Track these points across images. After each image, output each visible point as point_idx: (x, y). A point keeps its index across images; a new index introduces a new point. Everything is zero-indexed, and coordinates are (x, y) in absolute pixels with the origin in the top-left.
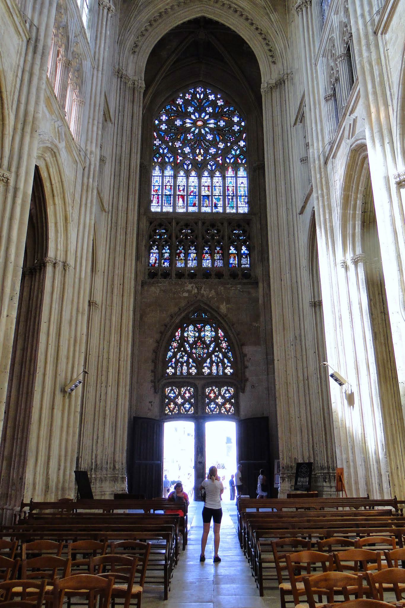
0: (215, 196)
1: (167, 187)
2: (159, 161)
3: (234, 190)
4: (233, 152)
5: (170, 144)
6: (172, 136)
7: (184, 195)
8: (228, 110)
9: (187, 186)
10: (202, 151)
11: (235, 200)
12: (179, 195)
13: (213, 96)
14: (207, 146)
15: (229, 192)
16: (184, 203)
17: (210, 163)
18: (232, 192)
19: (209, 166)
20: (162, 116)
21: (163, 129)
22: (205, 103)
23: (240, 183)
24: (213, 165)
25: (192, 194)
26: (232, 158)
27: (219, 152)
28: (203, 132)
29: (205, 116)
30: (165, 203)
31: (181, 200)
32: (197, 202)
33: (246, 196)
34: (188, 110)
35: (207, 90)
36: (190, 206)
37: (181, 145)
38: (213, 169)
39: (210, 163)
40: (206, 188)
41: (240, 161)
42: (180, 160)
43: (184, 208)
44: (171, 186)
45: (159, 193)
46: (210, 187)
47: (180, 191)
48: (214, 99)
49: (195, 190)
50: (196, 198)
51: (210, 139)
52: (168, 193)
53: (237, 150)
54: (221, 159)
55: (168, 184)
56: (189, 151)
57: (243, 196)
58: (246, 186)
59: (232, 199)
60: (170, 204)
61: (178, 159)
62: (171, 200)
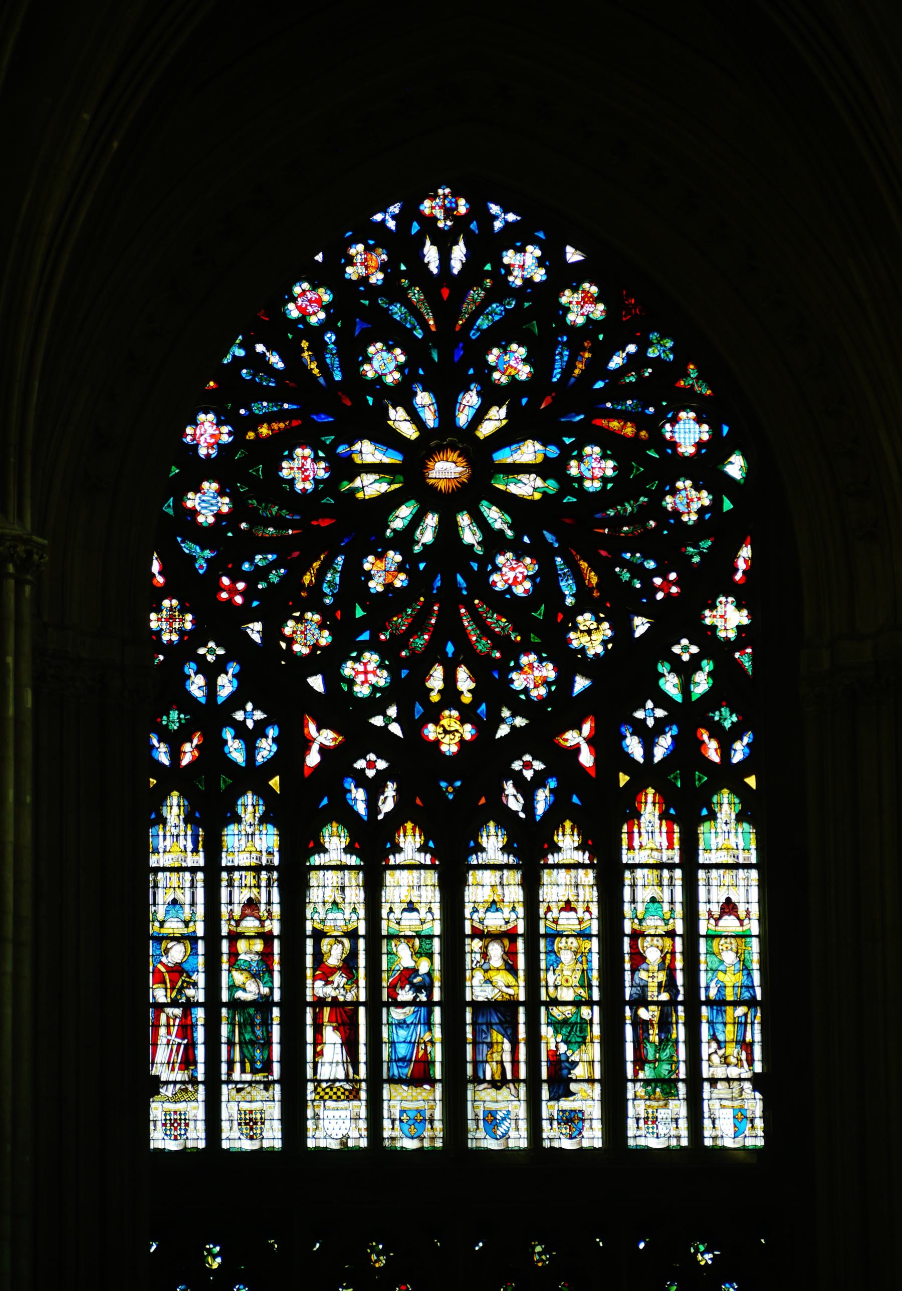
0: (555, 1002)
1: (242, 945)
2: (186, 760)
3: (679, 964)
4: (670, 685)
5: (255, 631)
6: (261, 573)
7: (356, 1004)
8: (633, 362)
9: (375, 937)
10: (465, 682)
11: (680, 1032)
12: (320, 1003)
13: (533, 252)
14: (499, 641)
15: (643, 975)
16: (355, 1063)
17: (517, 765)
18: (662, 977)
19: (509, 788)
20: (195, 423)
21: (206, 518)
22: (480, 310)
23: (716, 909)
24: (540, 780)
25: (405, 995)
26: (661, 726)
27: (581, 684)
28: (470, 536)
29: (479, 417)
30: (231, 1063)
31: (331, 1036)
32: (437, 1053)
33: (751, 1003)
34: (369, 372)
35: (495, 209)
36: (392, 1081)
37: (325, 638)
38: (540, 808)
39: (517, 765)
40: (496, 951)
41: (712, 750)
42: (323, 749)
43: (353, 1095)
44: (267, 938)
45: (190, 992)
46: (520, 945)
47: (325, 973)
48: (539, 275)
49: (424, 966)
50: (429, 1025)
51: (519, 590)
52: (251, 991)
53: (695, 664)
54: (589, 741)
55: (250, 925)
56: (382, 679)
57: (735, 1004)
58: (754, 927)
59: (665, 1025)
60: (267, 1067)
61: (308, 743)
62: (269, 1043)
